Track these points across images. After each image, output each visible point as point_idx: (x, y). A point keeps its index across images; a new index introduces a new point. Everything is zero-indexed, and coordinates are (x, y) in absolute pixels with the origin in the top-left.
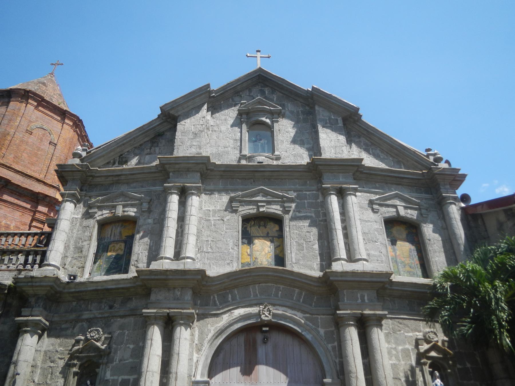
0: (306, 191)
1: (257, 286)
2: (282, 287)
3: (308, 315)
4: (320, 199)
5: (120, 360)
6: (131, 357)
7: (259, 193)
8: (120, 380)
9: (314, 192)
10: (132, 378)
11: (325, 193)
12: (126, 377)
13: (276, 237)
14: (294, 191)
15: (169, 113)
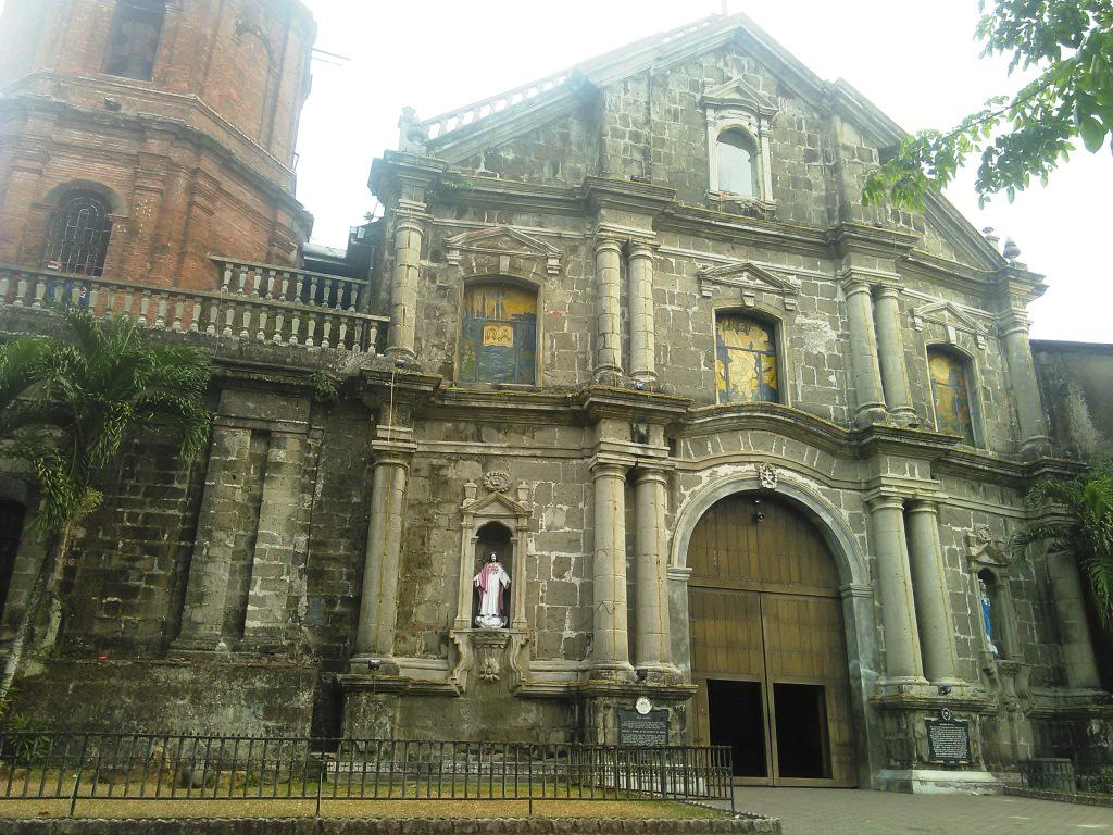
0: (816, 278)
1: (749, 433)
2: (786, 439)
3: (826, 488)
4: (840, 297)
5: (549, 528)
6: (567, 523)
7: (742, 271)
8: (553, 558)
9: (829, 283)
10: (573, 556)
11: (850, 285)
12: (563, 554)
13: (764, 353)
14: (799, 276)
15: (587, 81)
